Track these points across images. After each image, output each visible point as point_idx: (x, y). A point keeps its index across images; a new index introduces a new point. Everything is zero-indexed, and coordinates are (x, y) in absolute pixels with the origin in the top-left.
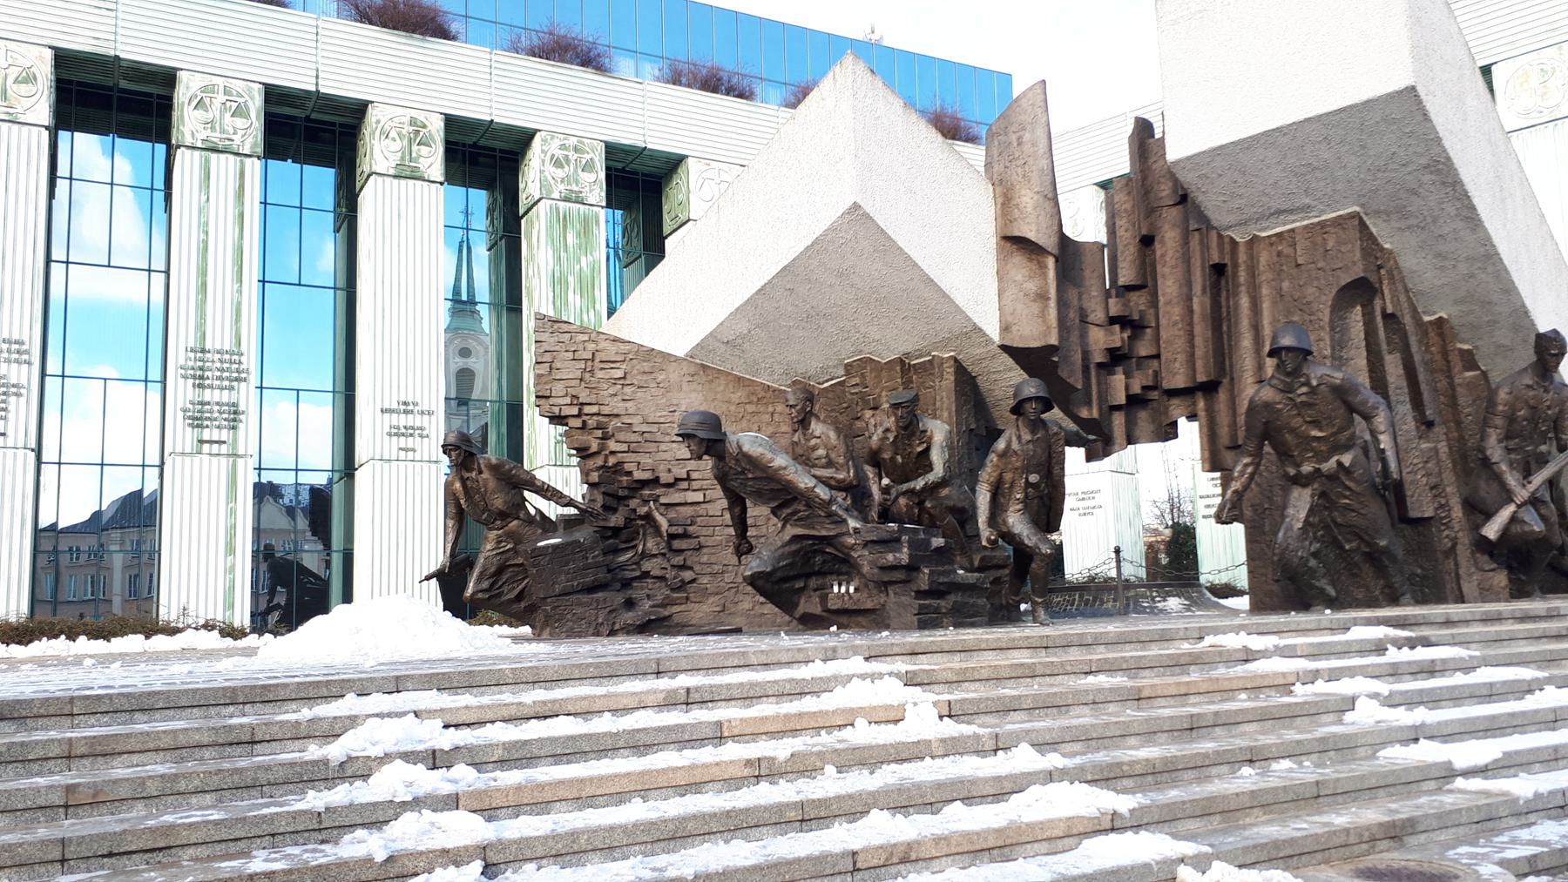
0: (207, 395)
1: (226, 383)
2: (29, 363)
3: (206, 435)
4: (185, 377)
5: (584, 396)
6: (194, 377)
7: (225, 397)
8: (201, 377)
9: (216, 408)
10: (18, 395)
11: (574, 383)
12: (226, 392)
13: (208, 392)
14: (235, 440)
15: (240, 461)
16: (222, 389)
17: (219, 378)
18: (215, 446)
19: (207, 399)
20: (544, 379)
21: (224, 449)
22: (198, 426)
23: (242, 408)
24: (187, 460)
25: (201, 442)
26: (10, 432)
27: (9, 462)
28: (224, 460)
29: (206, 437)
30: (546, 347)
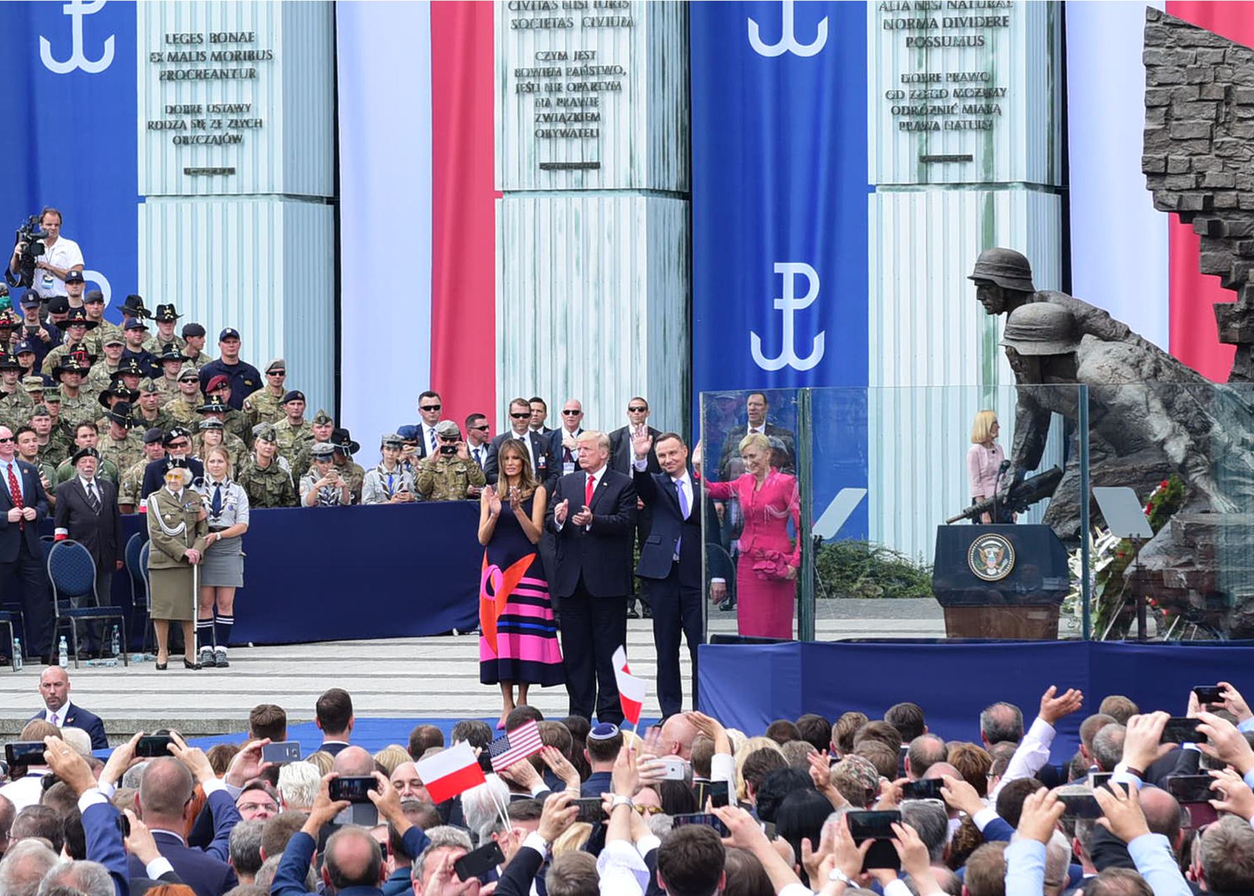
0: (938, 62)
1: (971, 32)
2: (630, 24)
3: (938, 145)
4: (892, 26)
5: (1214, 176)
6: (909, 25)
7: (970, 62)
8: (923, 25)
9: (953, 87)
10: (616, 88)
11: (1200, 147)
12: (971, 52)
13: (937, 54)
14: (989, 155)
15: (1001, 195)
16: (962, 44)
17: (957, 23)
18: (954, 166)
19: (936, 68)
20: (1157, 140)
21: (972, 172)
22: (924, 128)
23: (1002, 82)
24: (904, 196)
25: (926, 160)
26: (607, 163)
27: (608, 218)
28: (970, 195)
29: (937, 151)
30: (1161, 76)
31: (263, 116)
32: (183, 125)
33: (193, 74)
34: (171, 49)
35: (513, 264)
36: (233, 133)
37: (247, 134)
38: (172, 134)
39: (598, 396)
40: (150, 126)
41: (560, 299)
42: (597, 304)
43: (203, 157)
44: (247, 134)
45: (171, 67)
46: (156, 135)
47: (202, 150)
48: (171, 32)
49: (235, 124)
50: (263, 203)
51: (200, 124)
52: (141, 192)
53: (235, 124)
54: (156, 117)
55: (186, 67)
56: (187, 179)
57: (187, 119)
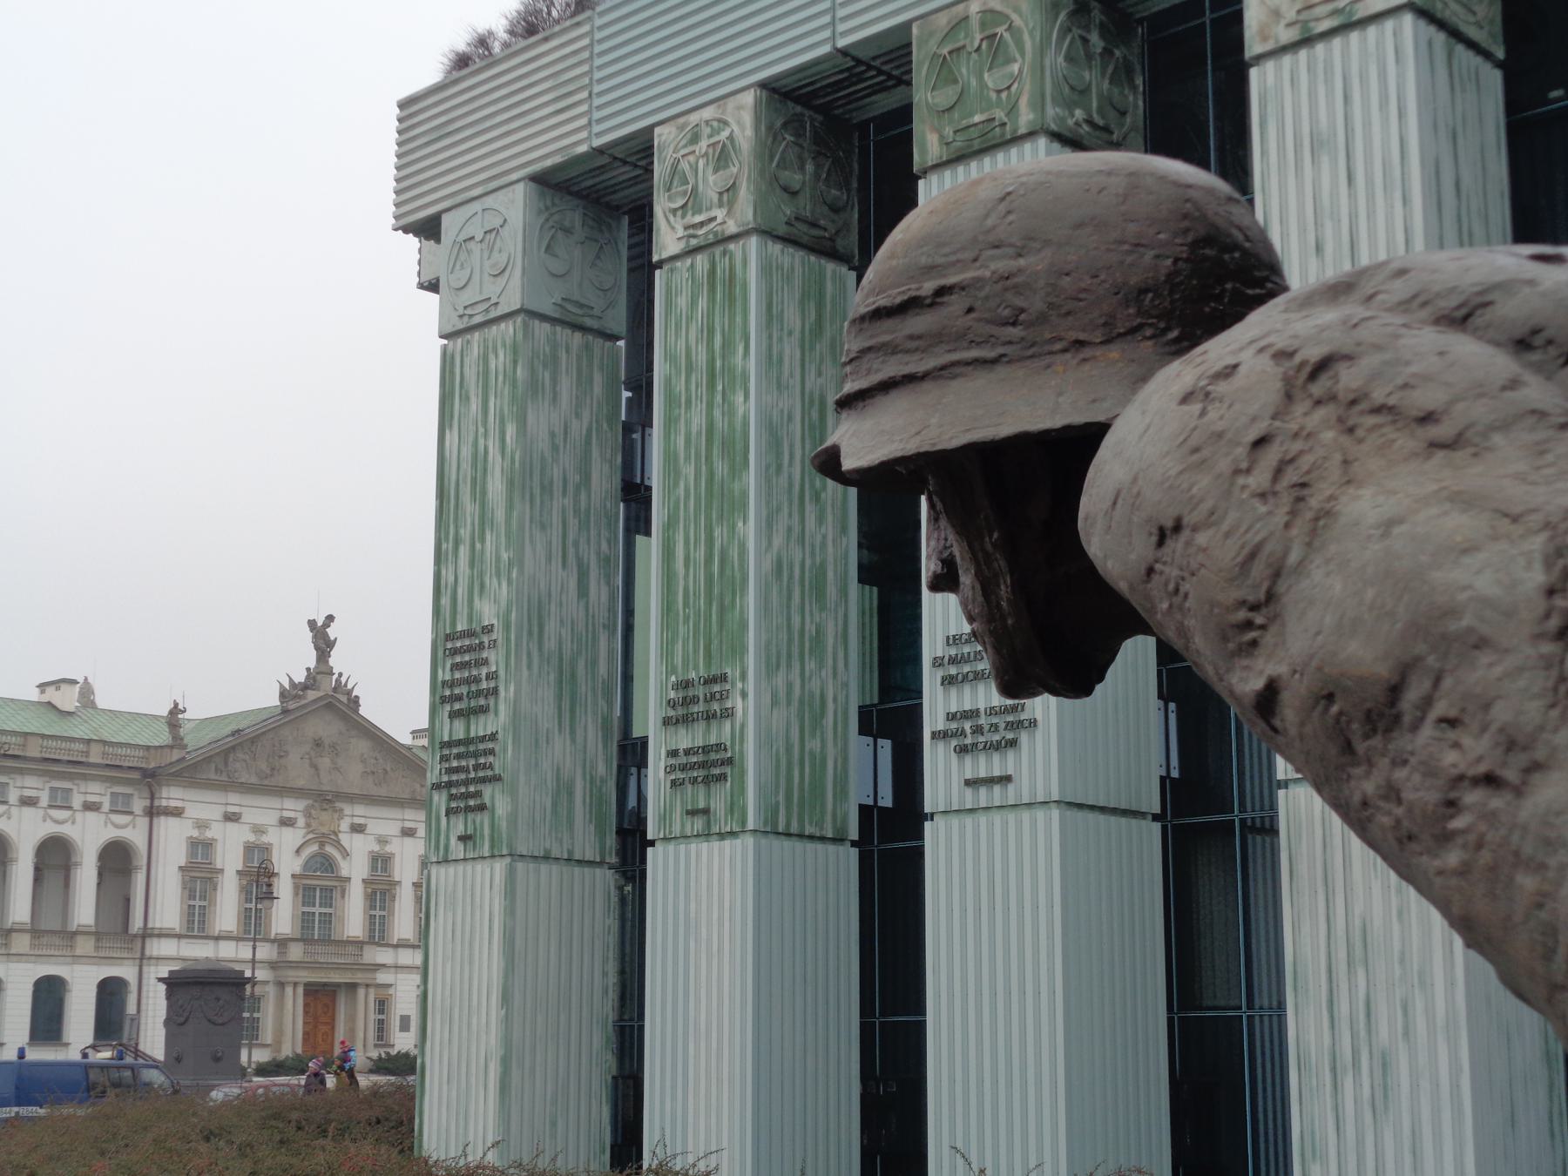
31: (1039, 716)
32: (963, 734)
33: (971, 676)
34: (953, 652)
35: (1303, 868)
36: (1010, 736)
37: (1024, 737)
38: (954, 743)
39: (1406, 1033)
40: (934, 735)
41: (1358, 909)
42: (1400, 914)
43: (983, 766)
44: (1024, 737)
45: (953, 671)
46: (941, 745)
47: (982, 759)
48: (952, 632)
49: (1010, 726)
50: (1040, 814)
51: (978, 730)
52: (927, 809)
53: (1010, 726)
54: (941, 725)
55: (966, 669)
56: (969, 792)
57: (967, 726)
